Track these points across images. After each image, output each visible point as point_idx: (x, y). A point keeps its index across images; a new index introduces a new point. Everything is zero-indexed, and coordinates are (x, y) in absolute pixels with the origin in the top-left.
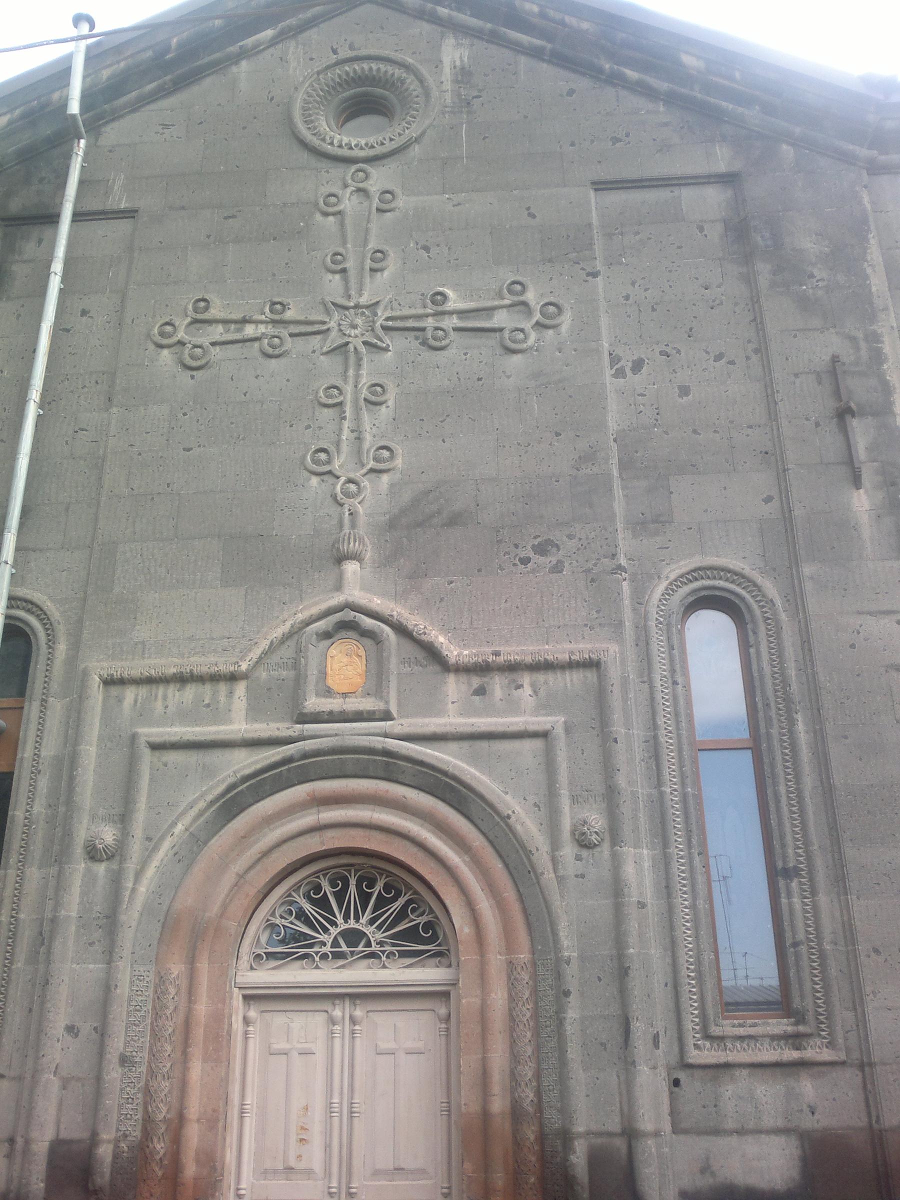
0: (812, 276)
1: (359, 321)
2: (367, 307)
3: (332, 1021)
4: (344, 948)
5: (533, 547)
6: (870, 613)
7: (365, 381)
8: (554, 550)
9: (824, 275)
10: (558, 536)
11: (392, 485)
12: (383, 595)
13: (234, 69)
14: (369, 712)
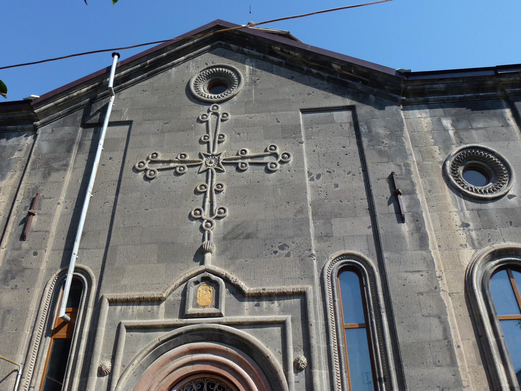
0: (383, 142)
1: (213, 161)
2: (217, 155)
5: (279, 247)
6: (410, 272)
7: (214, 183)
8: (287, 247)
9: (387, 142)
10: (288, 242)
11: (224, 223)
12: (220, 266)
13: (170, 71)
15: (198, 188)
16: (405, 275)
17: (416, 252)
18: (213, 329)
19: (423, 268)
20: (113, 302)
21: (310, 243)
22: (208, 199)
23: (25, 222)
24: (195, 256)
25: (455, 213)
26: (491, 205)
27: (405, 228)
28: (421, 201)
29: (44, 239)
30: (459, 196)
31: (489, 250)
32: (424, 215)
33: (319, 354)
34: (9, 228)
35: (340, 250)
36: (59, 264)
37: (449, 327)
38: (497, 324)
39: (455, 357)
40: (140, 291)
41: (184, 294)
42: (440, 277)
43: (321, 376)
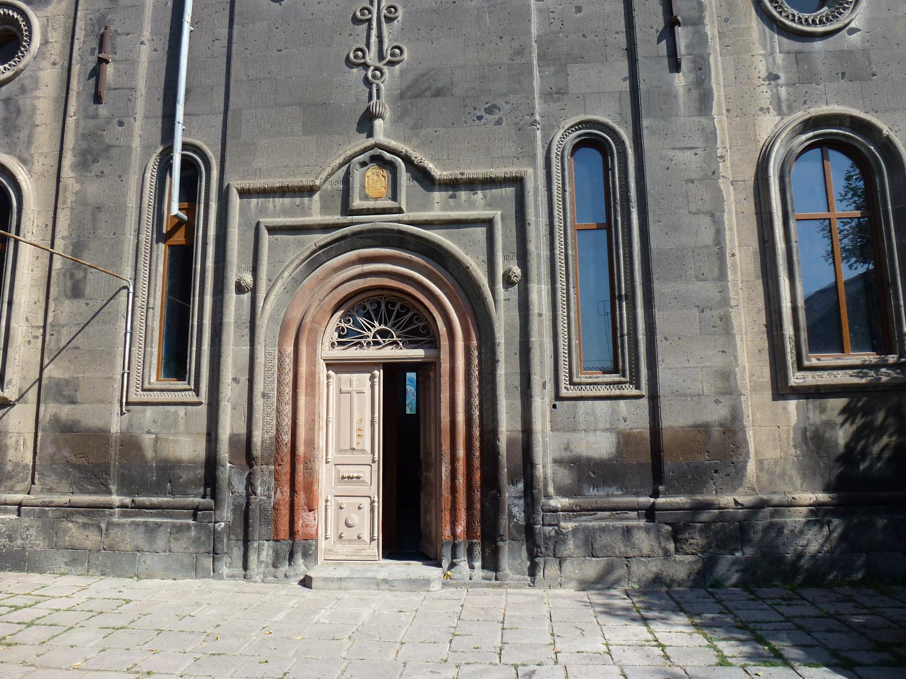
4: (379, 339)
5: (485, 109)
6: (679, 149)
8: (497, 111)
10: (500, 102)
11: (401, 71)
12: (397, 139)
14: (389, 209)
15: (358, 14)
16: (671, 153)
17: (692, 119)
18: (391, 231)
19: (698, 142)
20: (244, 193)
21: (533, 104)
22: (374, 32)
23: (96, 74)
24: (359, 124)
25: (760, 58)
26: (818, 45)
27: (680, 80)
28: (710, 36)
29: (129, 100)
30: (772, 29)
31: (801, 117)
32: (712, 60)
33: (539, 264)
34: (74, 84)
35: (577, 114)
36: (159, 138)
37: (724, 229)
38: (792, 224)
39: (726, 268)
40: (282, 177)
41: (346, 180)
42: (721, 157)
43: (539, 292)
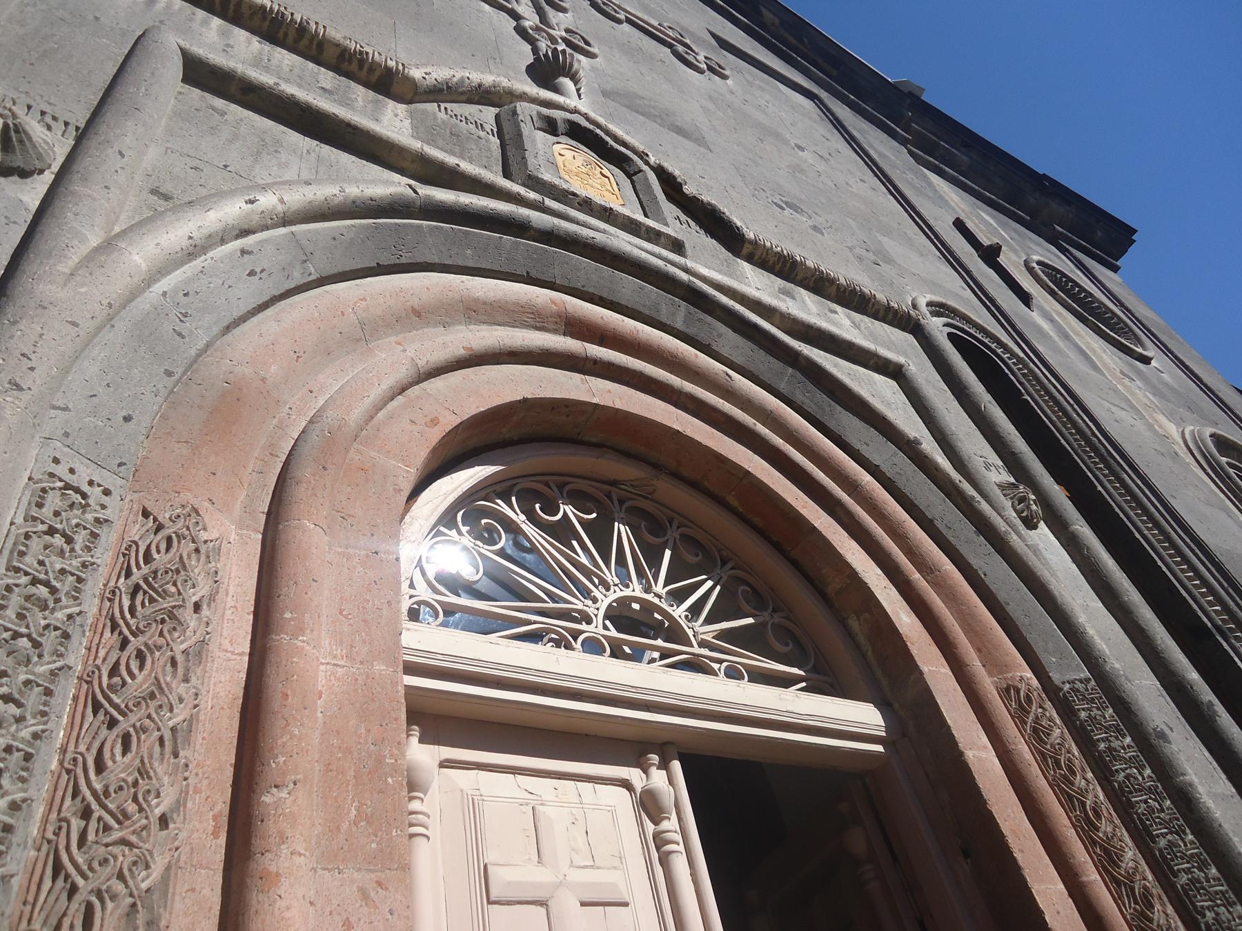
3: (649, 805)
